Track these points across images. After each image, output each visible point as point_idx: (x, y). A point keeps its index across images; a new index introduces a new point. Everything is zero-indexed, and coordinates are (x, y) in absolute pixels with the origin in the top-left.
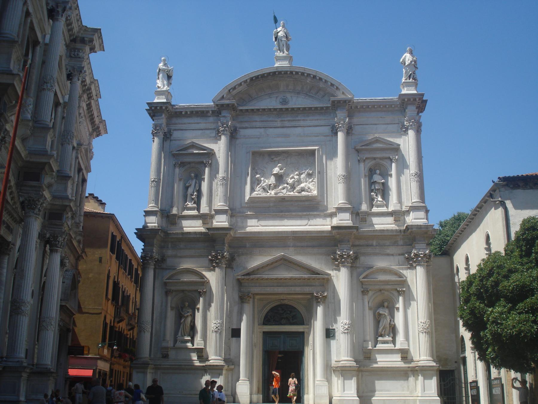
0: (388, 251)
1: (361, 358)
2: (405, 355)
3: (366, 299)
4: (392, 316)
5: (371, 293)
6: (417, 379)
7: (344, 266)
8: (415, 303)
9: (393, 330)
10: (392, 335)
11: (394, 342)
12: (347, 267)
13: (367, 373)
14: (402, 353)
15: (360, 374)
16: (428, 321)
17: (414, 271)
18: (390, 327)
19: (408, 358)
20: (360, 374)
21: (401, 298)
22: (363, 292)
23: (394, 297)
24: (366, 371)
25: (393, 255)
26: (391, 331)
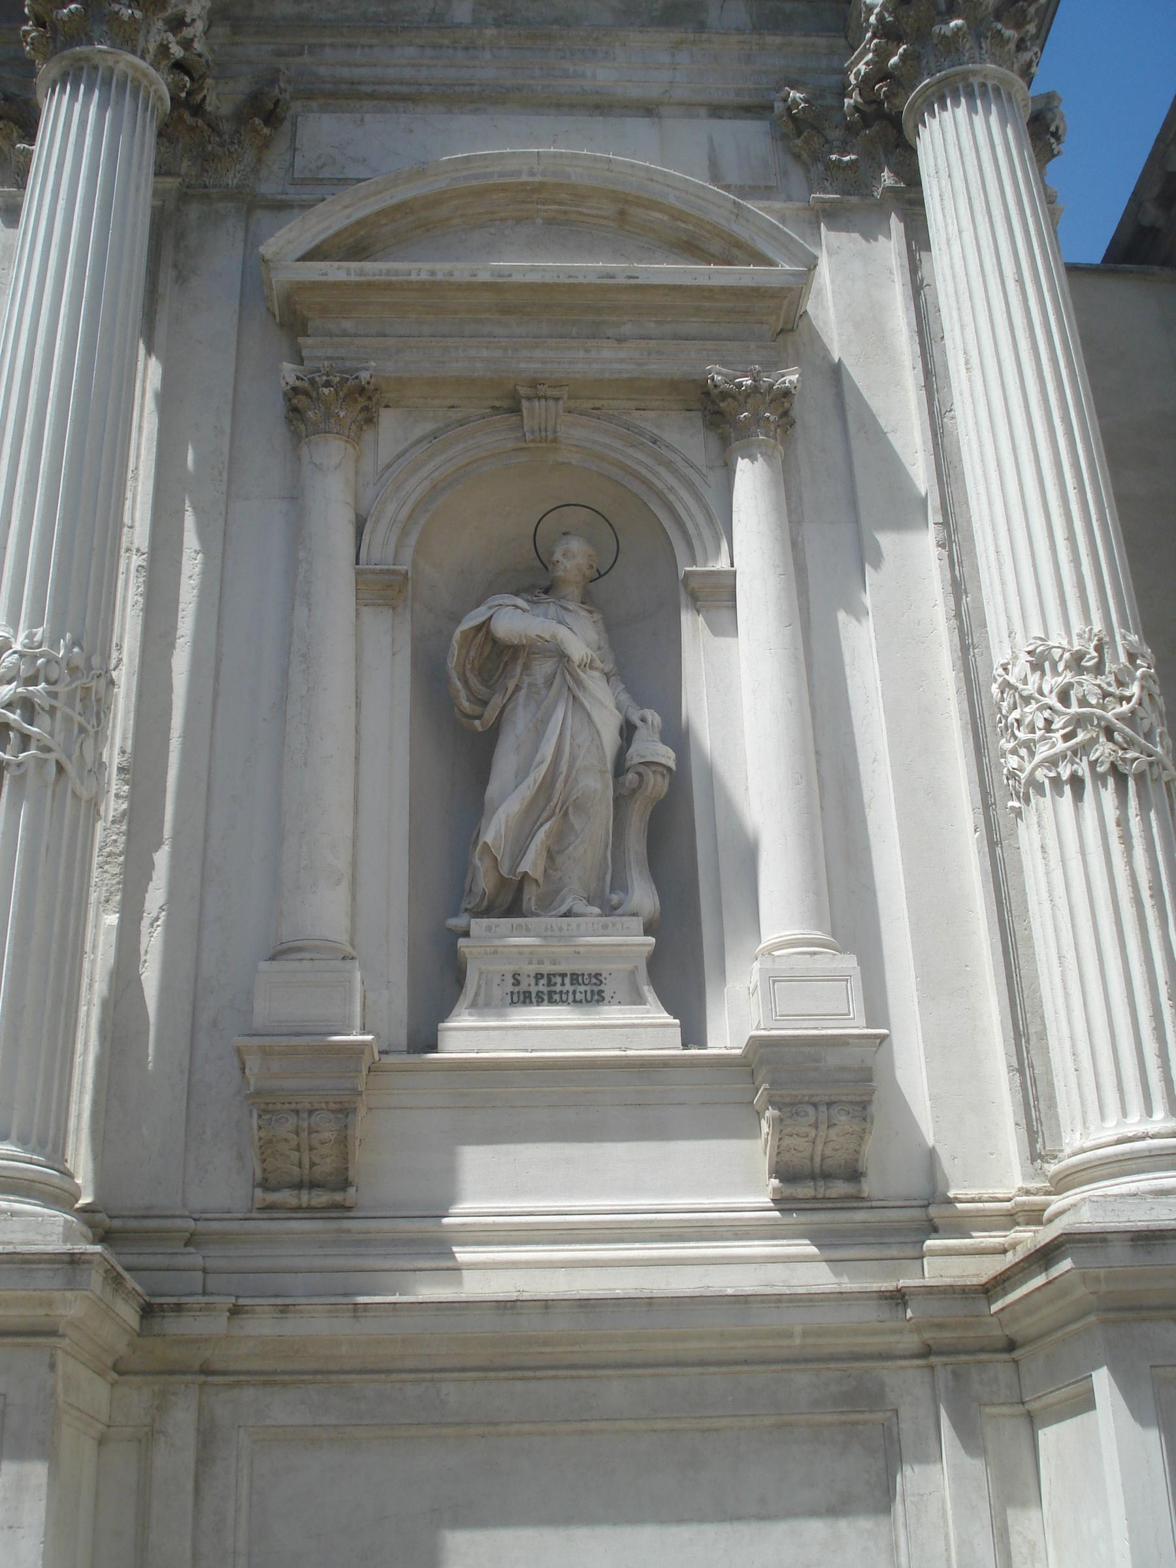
0: (602, 75)
1: (221, 1185)
2: (833, 1143)
3: (334, 479)
4: (649, 672)
5: (392, 430)
6: (1016, 1486)
7: (72, 76)
8: (925, 546)
9: (666, 834)
10: (643, 896)
11: (679, 973)
12: (110, 85)
13: (283, 1409)
14: (789, 1109)
15: (182, 1418)
16: (1125, 639)
17: (891, 246)
18: (621, 801)
19: (868, 1187)
20: (182, 1418)
21: (750, 482)
22: (301, 411)
23: (665, 479)
24: (268, 1379)
25: (648, 109)
26: (636, 844)
